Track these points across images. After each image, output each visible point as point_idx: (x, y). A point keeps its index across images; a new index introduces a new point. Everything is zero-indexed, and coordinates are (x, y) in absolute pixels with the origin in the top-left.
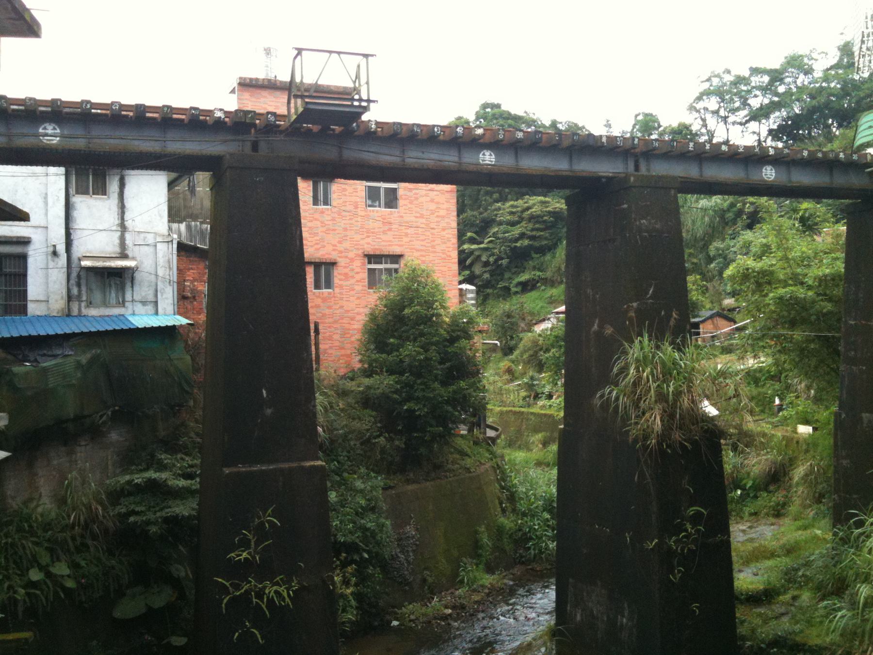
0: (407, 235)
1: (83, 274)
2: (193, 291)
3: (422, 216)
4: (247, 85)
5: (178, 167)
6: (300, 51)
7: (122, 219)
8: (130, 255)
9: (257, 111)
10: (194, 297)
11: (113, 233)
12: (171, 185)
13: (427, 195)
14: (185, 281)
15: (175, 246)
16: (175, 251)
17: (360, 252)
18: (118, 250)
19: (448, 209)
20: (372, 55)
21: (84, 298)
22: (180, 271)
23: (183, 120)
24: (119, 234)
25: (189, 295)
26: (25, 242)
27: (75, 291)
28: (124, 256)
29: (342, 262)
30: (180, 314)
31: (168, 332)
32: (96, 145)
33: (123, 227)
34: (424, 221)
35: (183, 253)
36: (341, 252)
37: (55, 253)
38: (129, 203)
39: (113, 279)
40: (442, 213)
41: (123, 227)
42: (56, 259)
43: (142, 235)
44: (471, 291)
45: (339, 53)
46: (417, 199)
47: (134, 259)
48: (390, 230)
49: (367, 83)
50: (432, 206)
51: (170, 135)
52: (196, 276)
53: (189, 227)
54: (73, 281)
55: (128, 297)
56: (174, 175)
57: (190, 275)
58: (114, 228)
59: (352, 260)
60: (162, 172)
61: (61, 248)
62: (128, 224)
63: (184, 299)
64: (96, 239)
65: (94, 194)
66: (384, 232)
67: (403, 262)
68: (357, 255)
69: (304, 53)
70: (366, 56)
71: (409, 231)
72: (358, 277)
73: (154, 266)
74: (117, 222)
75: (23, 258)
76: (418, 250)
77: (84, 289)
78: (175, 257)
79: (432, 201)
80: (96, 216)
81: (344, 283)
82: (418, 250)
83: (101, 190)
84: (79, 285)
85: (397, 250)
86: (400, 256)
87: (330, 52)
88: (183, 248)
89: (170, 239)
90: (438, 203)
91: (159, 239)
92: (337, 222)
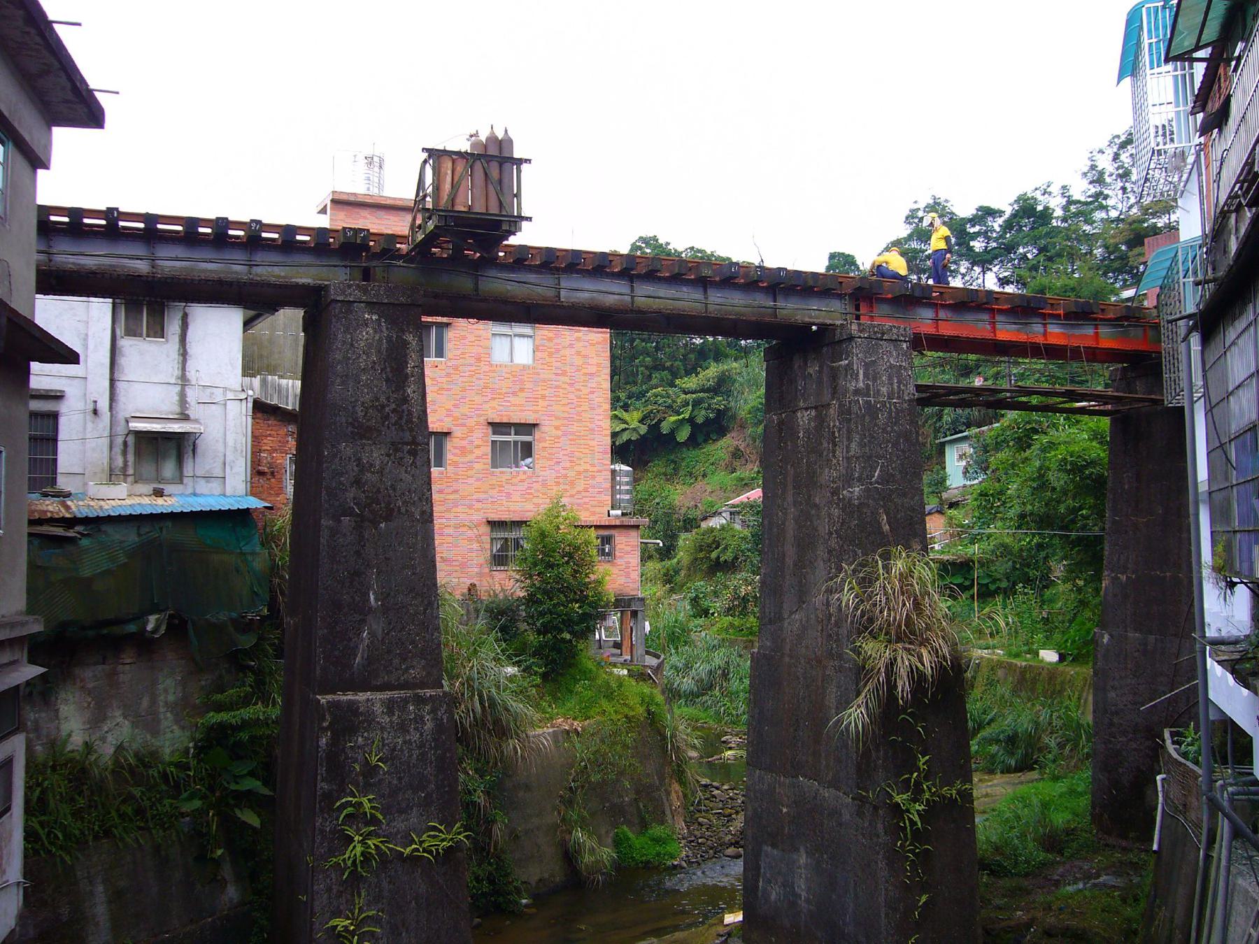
0: (543, 397)
1: (131, 440)
2: (271, 466)
3: (564, 373)
4: (340, 202)
5: (256, 301)
7: (184, 369)
8: (192, 417)
10: (272, 473)
11: (170, 387)
12: (247, 324)
13: (571, 346)
14: (260, 451)
15: (250, 405)
17: (482, 419)
18: (178, 409)
19: (598, 365)
20: (528, 161)
21: (131, 471)
22: (255, 438)
23: (273, 240)
24: (178, 388)
25: (266, 469)
26: (58, 397)
27: (119, 461)
28: (185, 417)
29: (458, 432)
30: (253, 494)
31: (242, 516)
32: (158, 271)
33: (184, 380)
34: (567, 379)
35: (259, 415)
36: (456, 419)
37: (95, 412)
38: (193, 348)
39: (163, 449)
40: (593, 369)
41: (184, 380)
42: (98, 420)
43: (209, 390)
44: (627, 474)
46: (558, 351)
47: (196, 421)
48: (522, 390)
50: (578, 361)
51: (259, 257)
52: (276, 445)
53: (264, 383)
54: (118, 449)
55: (188, 469)
56: (251, 313)
57: (268, 443)
58: (173, 381)
59: (471, 431)
61: (104, 405)
62: (191, 375)
63: (260, 473)
64: (149, 395)
65: (148, 336)
66: (514, 394)
67: (537, 434)
68: (478, 424)
71: (546, 393)
72: (478, 452)
73: (222, 430)
74: (177, 373)
75: (55, 416)
76: (558, 418)
77: (131, 458)
78: (250, 419)
79: (578, 353)
80: (150, 361)
81: (462, 460)
82: (558, 418)
83: (158, 330)
84: (125, 453)
86: (535, 425)
88: (261, 409)
89: (243, 396)
90: (585, 356)
91: (230, 395)
92: (482, 370)
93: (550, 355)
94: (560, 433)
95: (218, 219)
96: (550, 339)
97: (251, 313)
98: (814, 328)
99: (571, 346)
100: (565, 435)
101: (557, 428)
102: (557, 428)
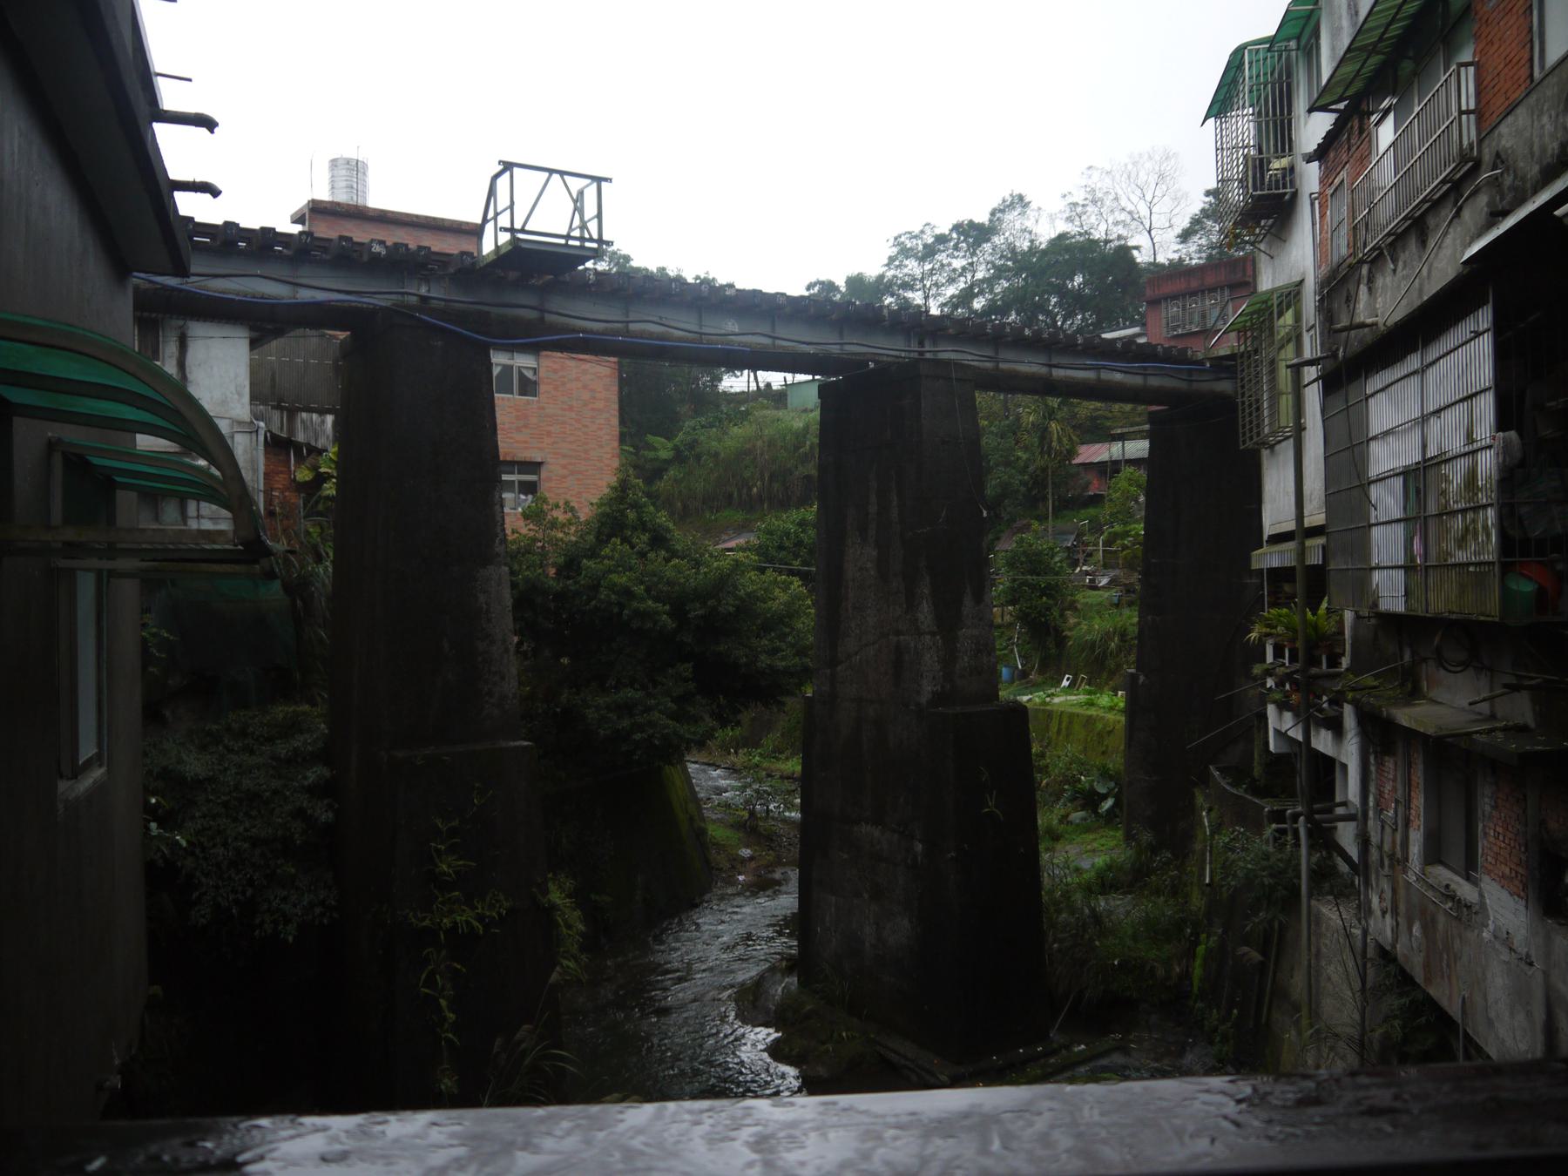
0: (549, 434)
3: (571, 408)
5: (264, 324)
6: (508, 166)
9: (434, 249)
12: (254, 344)
13: (577, 379)
15: (261, 438)
16: (261, 447)
20: (606, 180)
34: (573, 415)
40: (599, 405)
45: (562, 173)
46: (564, 384)
48: (526, 426)
49: (599, 216)
50: (586, 395)
56: (255, 334)
60: (227, 330)
66: (518, 429)
67: (544, 473)
69: (516, 170)
70: (599, 180)
76: (564, 456)
79: (585, 387)
82: (564, 456)
85: (537, 457)
86: (540, 464)
87: (551, 171)
90: (593, 390)
93: (556, 388)
94: (565, 472)
95: (263, 229)
96: (555, 371)
97: (255, 334)
98: (871, 365)
99: (577, 379)
100: (573, 473)
101: (564, 467)
102: (564, 467)
